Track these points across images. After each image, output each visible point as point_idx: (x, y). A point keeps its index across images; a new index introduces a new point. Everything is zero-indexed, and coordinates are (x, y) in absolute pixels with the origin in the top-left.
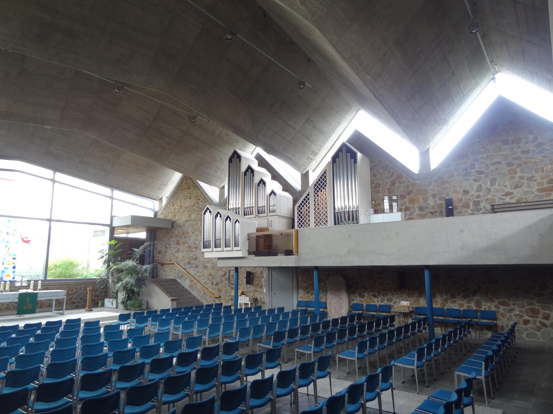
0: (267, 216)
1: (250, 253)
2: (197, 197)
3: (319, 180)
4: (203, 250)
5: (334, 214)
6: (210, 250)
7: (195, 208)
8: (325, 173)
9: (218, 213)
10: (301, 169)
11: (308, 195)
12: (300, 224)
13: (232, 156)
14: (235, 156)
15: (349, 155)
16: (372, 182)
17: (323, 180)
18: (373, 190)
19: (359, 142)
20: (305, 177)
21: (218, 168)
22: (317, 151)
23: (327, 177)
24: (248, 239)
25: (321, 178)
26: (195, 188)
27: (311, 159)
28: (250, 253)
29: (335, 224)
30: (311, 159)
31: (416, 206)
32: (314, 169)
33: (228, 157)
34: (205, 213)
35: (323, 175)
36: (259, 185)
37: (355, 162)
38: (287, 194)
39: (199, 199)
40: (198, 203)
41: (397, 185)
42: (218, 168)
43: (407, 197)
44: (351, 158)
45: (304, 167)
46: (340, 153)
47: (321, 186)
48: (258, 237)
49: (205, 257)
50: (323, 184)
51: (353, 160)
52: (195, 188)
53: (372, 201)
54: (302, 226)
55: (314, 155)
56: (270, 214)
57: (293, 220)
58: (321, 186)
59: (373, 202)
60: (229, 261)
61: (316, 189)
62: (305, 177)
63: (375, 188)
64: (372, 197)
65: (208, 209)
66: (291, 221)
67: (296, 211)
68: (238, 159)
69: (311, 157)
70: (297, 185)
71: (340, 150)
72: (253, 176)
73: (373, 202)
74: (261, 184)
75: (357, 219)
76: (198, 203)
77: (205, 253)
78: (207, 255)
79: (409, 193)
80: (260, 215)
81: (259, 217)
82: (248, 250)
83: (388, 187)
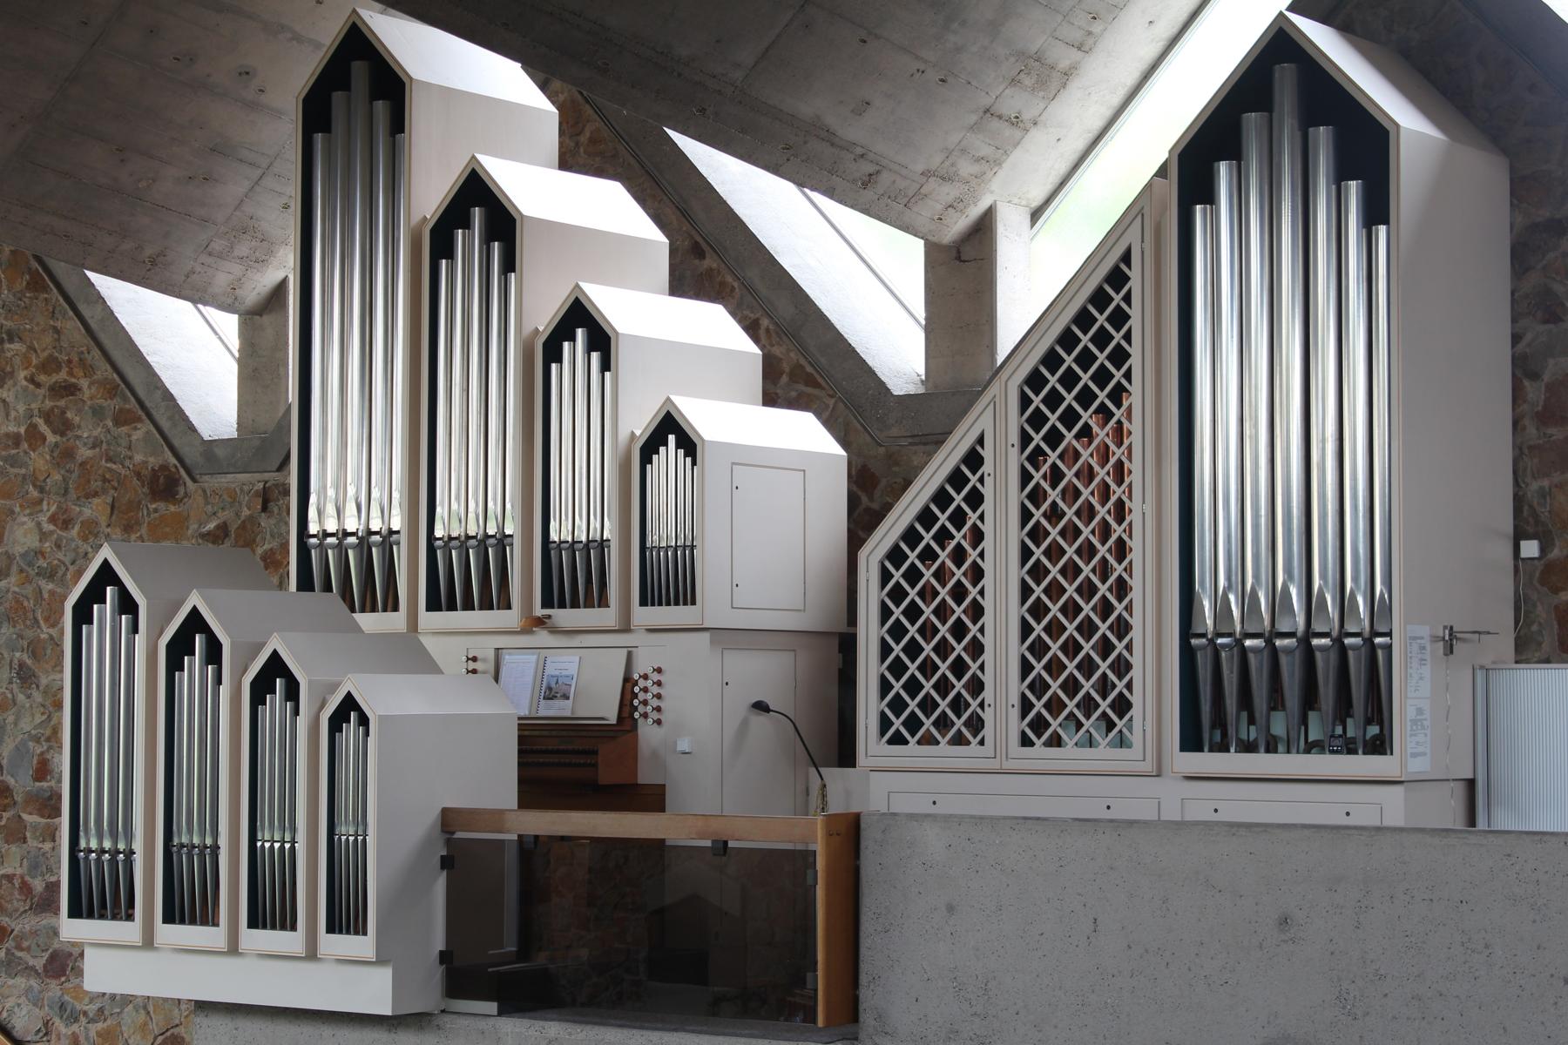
0: (626, 629)
1: (463, 976)
2: (50, 365)
3: (1068, 340)
4: (73, 930)
5: (1188, 655)
6: (128, 931)
7: (39, 460)
8: (1117, 278)
9: (195, 622)
10: (924, 213)
11: (973, 459)
12: (898, 705)
13: (332, 78)
14: (359, 71)
15: (1323, 137)
16: (1524, 368)
17: (1102, 339)
18: (1531, 430)
20: (962, 271)
21: (222, 149)
22: (1063, 56)
24: (446, 863)
25: (1083, 319)
26: (36, 285)
27: (1015, 121)
28: (463, 976)
29: (1191, 741)
30: (1015, 121)
32: (1037, 197)
34: (83, 615)
35: (1100, 298)
36: (552, 353)
37: (1376, 211)
38: (803, 434)
39: (70, 390)
40: (63, 426)
42: (222, 149)
44: (1341, 175)
45: (947, 192)
47: (1086, 398)
48: (531, 850)
50: (1102, 377)
51: (1353, 187)
52: (36, 285)
53: (1519, 536)
54: (913, 724)
55: (1041, 84)
56: (645, 616)
57: (847, 644)
58: (1086, 398)
59: (1530, 549)
61: (1037, 420)
62: (962, 271)
63: (1545, 417)
64: (1519, 501)
65: (106, 575)
66: (836, 660)
67: (870, 595)
68: (381, 107)
69: (1013, 101)
70: (897, 350)
71: (1249, 90)
72: (509, 265)
73: (1530, 549)
74: (576, 349)
75: (1379, 709)
76: (63, 426)
80: (565, 617)
81: (555, 631)
82: (444, 957)
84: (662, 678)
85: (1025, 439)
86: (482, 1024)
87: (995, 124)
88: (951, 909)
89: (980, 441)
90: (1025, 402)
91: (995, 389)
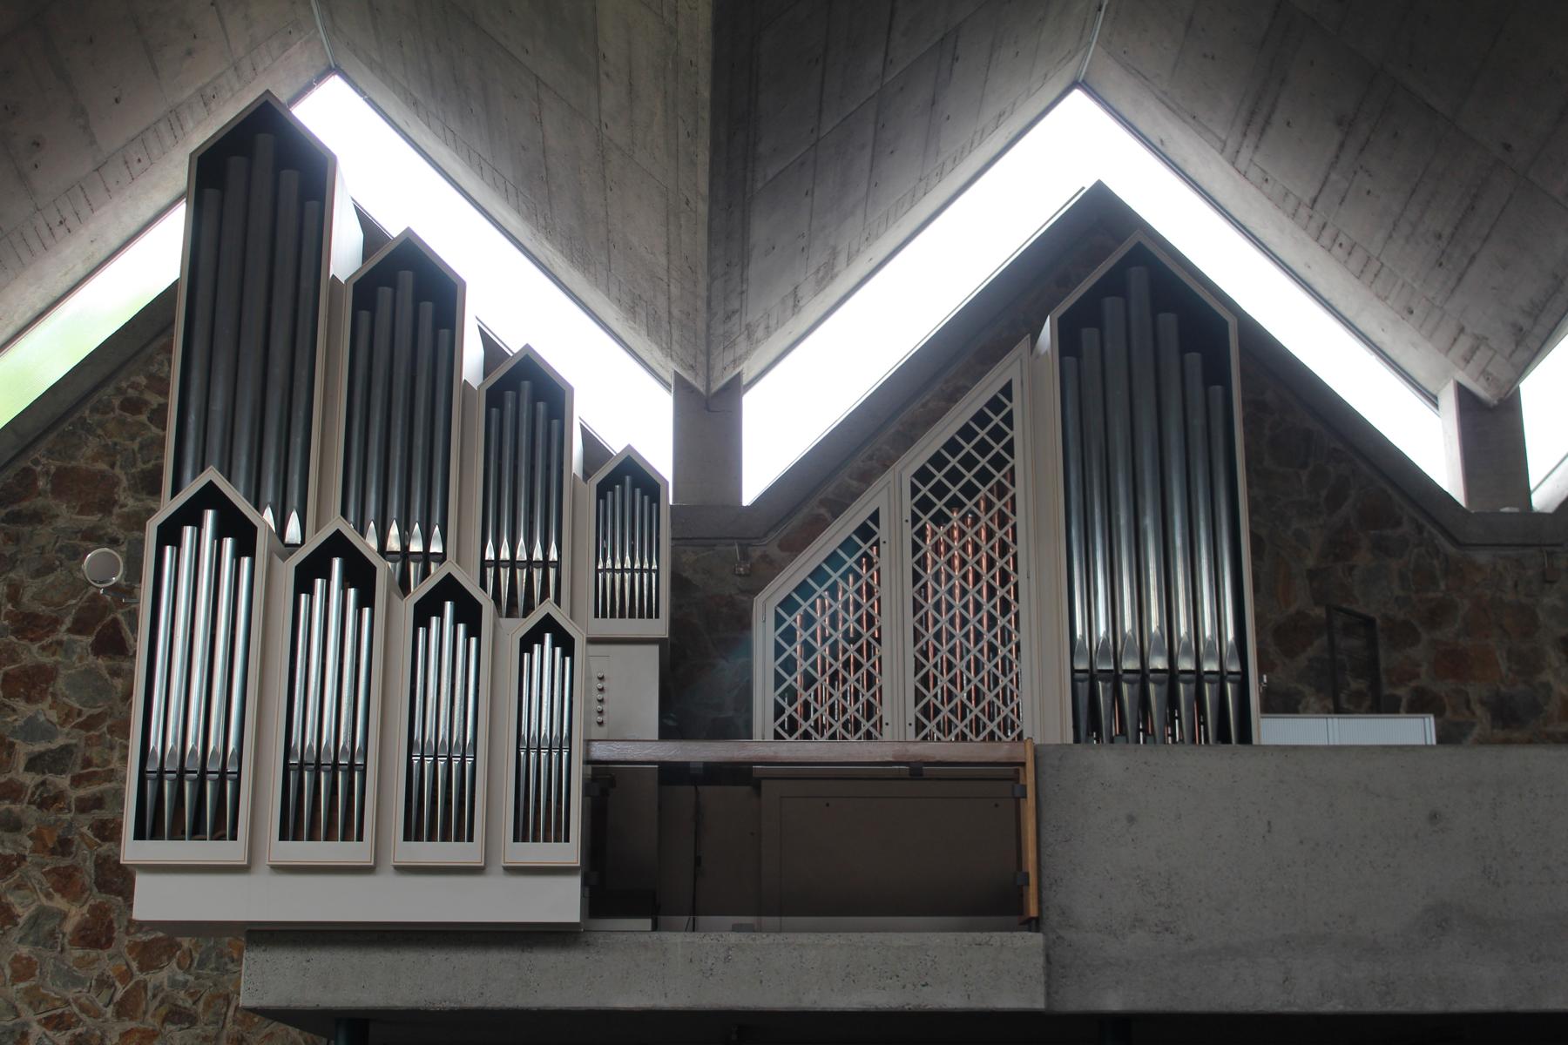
4: (133, 851)
5: (1074, 681)
11: (865, 532)
15: (1169, 320)
19: (1098, 274)
20: (708, 418)
23: (1017, 433)
31: (1476, 690)
33: (200, 135)
34: (169, 535)
41: (1363, 559)
43: (1425, 637)
44: (1183, 350)
46: (1111, 304)
49: (141, 912)
60: (407, 960)
77: (142, 882)
78: (155, 901)
79: (1437, 614)
83: (1310, 562)
84: (605, 684)
85: (915, 519)
86: (644, 938)
87: (790, 303)
88: (1131, 819)
89: (875, 517)
90: (915, 490)
91: (889, 476)
